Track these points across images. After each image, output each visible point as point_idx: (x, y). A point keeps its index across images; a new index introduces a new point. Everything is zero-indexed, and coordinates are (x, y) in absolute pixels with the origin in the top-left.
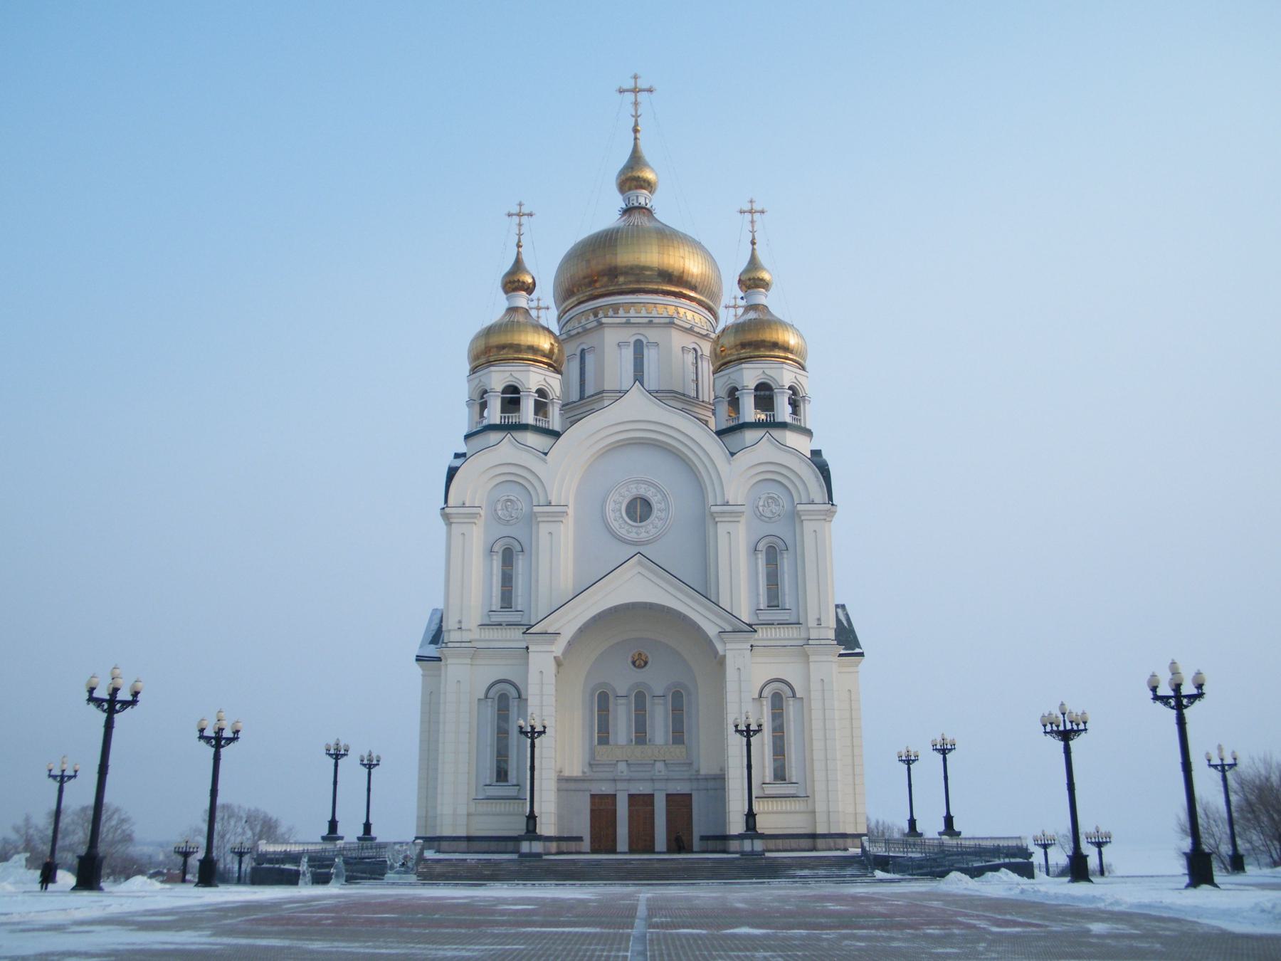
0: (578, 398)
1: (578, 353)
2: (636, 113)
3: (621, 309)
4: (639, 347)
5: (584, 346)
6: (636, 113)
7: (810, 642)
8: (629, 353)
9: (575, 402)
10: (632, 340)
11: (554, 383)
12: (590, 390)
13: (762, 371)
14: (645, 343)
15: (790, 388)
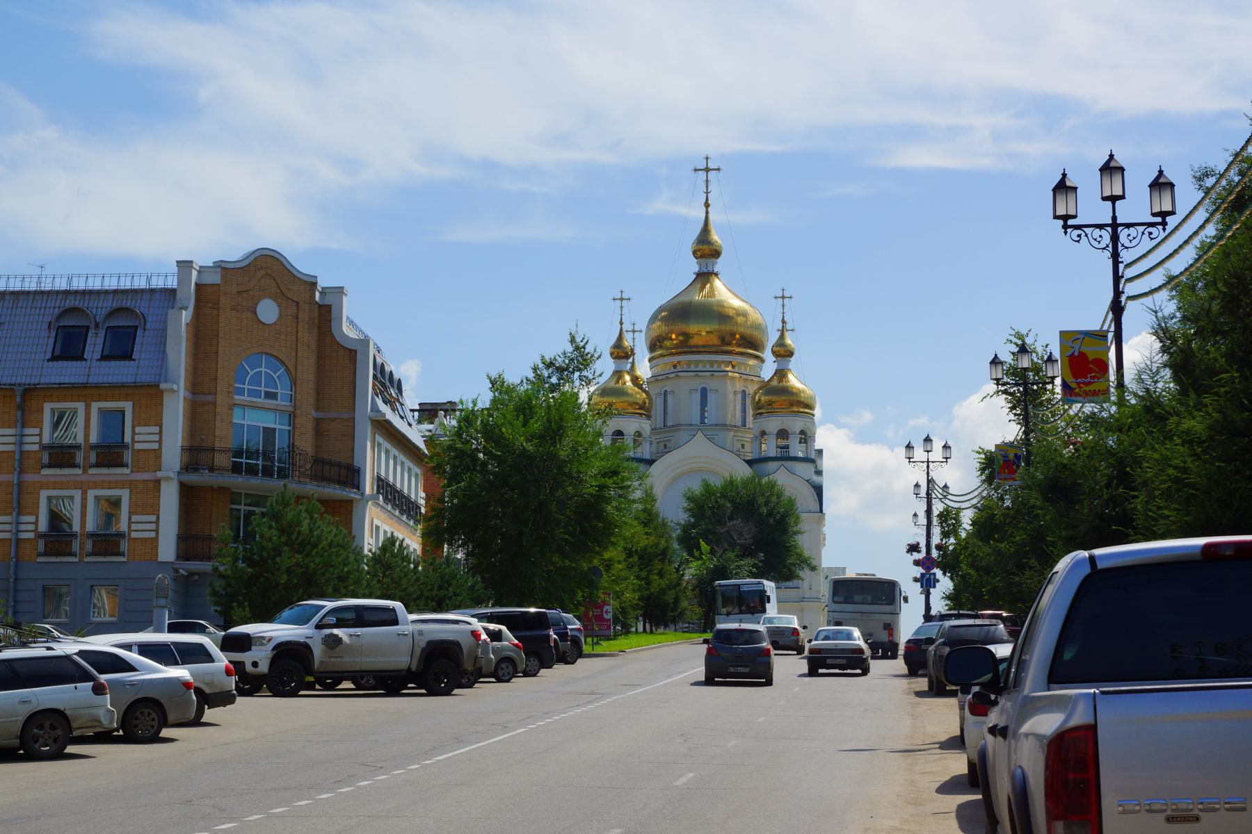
0: (662, 426)
1: (663, 392)
2: (707, 190)
3: (693, 364)
4: (704, 392)
5: (665, 388)
6: (707, 190)
7: (805, 600)
8: (697, 397)
9: (661, 428)
10: (700, 388)
11: (645, 426)
12: (669, 423)
13: (781, 422)
14: (708, 389)
15: (802, 432)
